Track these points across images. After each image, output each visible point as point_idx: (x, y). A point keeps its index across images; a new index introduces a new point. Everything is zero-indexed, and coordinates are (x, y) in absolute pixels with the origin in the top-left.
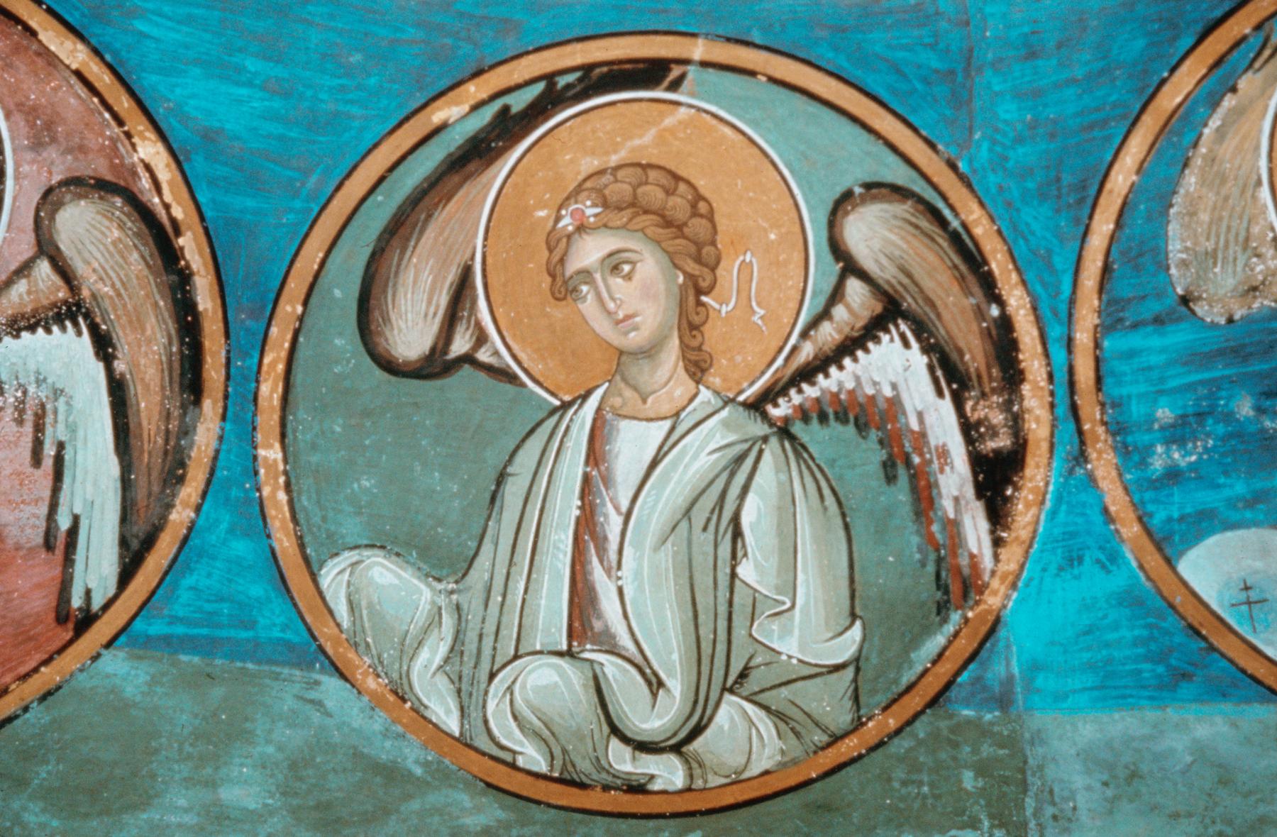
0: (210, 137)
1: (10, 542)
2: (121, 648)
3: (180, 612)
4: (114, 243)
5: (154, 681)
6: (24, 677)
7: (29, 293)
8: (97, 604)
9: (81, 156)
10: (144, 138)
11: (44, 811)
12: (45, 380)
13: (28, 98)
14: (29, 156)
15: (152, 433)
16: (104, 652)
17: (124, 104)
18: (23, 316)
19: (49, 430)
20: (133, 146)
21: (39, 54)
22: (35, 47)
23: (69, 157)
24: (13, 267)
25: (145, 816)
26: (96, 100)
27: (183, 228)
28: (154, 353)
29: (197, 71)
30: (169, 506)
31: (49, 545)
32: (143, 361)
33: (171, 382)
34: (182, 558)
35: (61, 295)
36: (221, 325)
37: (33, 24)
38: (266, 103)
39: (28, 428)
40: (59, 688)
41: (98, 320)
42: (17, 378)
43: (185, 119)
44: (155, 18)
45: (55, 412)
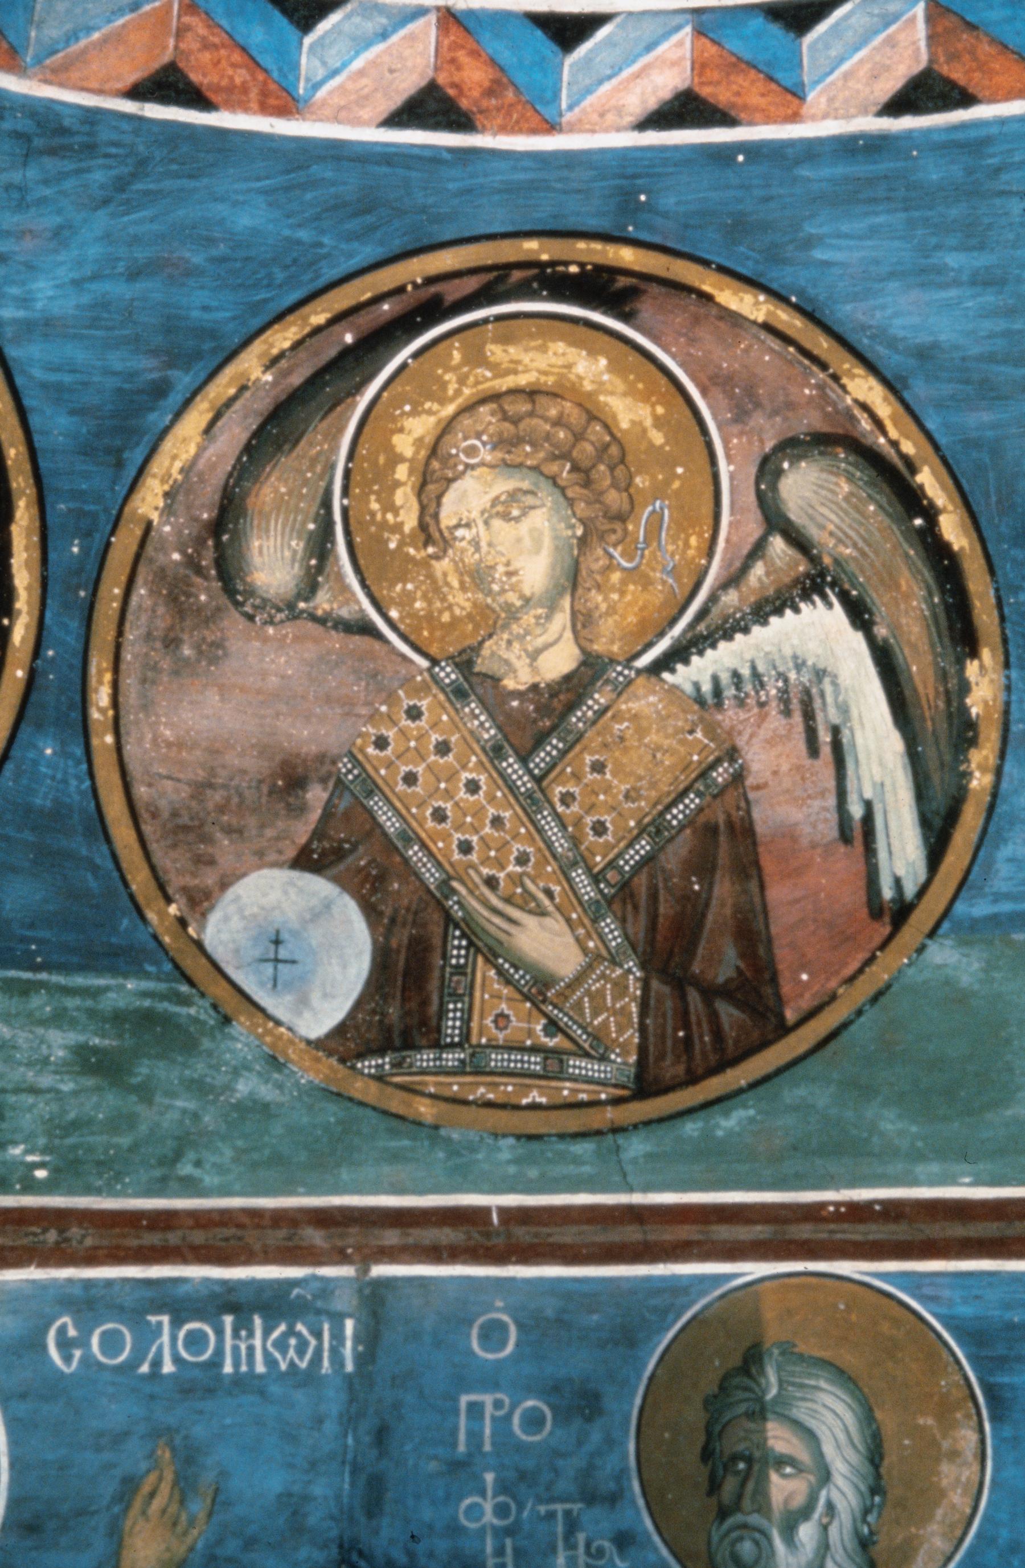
0: (925, 354)
1: (805, 842)
2: (946, 936)
3: (1003, 887)
4: (846, 499)
5: (990, 967)
6: (851, 980)
7: (768, 574)
8: (910, 890)
9: (790, 414)
10: (853, 376)
11: (900, 1116)
12: (804, 663)
13: (720, 368)
14: (735, 429)
15: (931, 697)
16: (929, 942)
17: (822, 345)
18: (767, 600)
19: (820, 717)
20: (843, 387)
21: (721, 318)
22: (714, 311)
23: (778, 419)
24: (745, 551)
25: (1009, 1113)
26: (791, 349)
27: (917, 463)
28: (914, 609)
29: (893, 285)
30: (967, 775)
31: (845, 836)
32: (904, 621)
33: (940, 636)
34: (992, 829)
35: (801, 569)
36: (982, 561)
37: (706, 288)
38: (979, 299)
39: (798, 718)
40: (888, 986)
41: (847, 586)
42: (775, 667)
43: (892, 343)
44: (834, 241)
45: (822, 695)
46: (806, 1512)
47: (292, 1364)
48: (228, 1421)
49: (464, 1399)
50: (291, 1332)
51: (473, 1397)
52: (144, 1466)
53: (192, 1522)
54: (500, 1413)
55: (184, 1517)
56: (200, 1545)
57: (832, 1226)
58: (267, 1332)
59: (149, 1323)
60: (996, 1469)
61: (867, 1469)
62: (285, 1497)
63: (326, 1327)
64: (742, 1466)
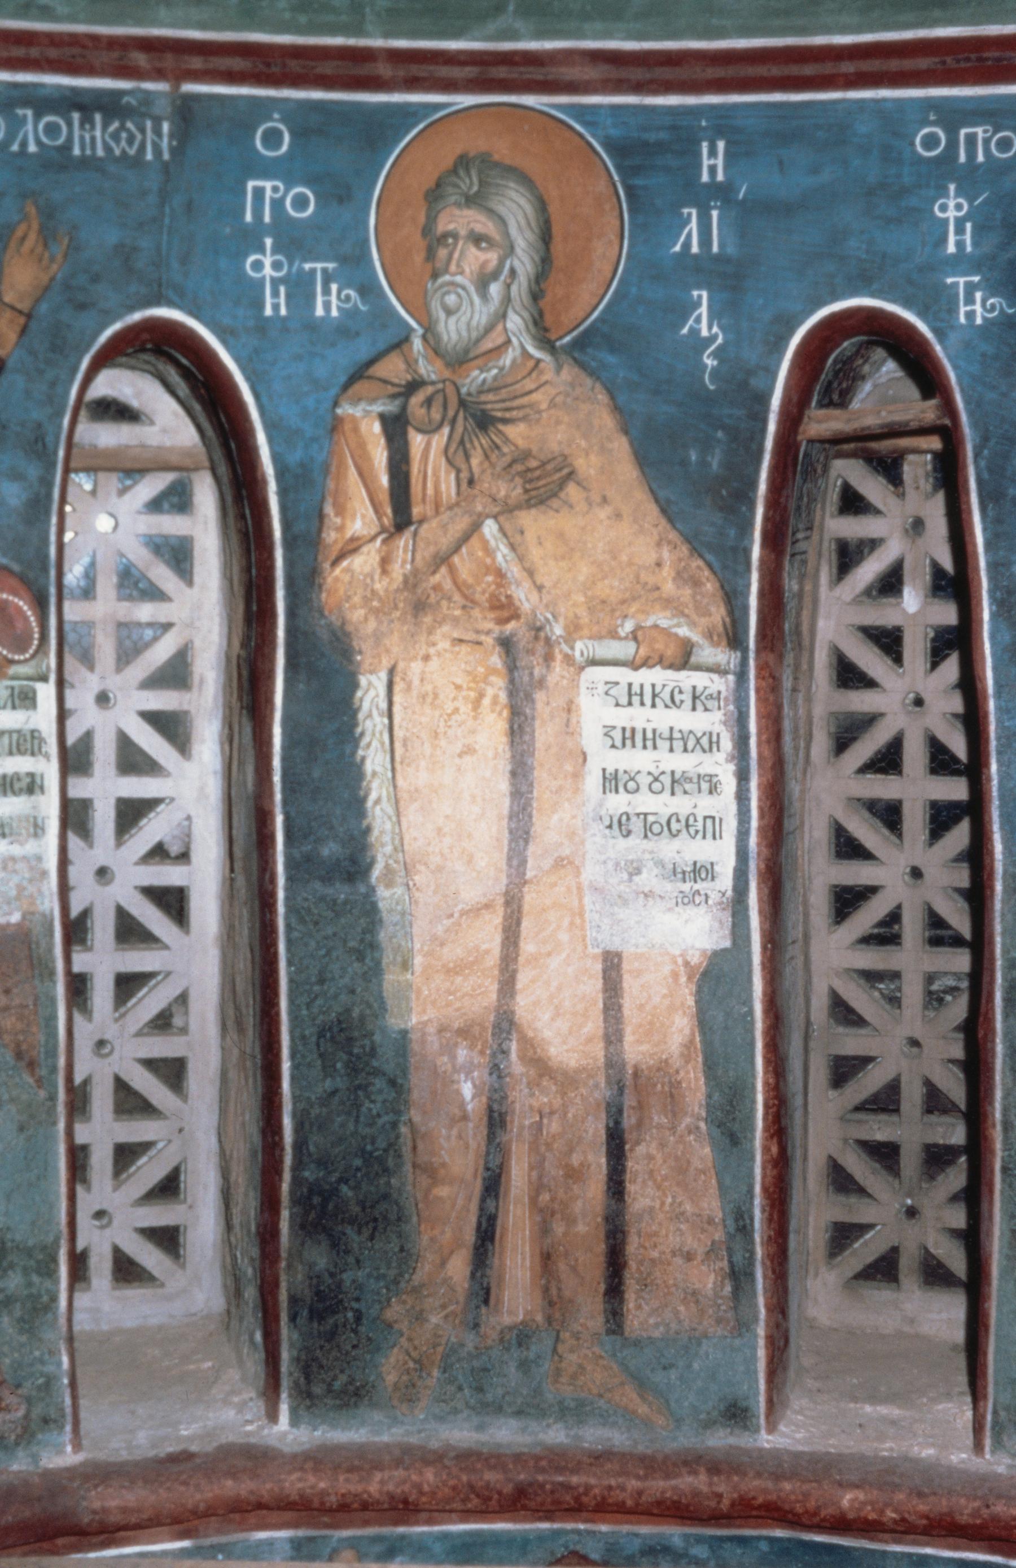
46: (495, 276)
47: (124, 152)
48: (77, 189)
49: (251, 184)
50: (122, 127)
51: (259, 183)
52: (16, 218)
53: (52, 259)
54: (277, 196)
55: (47, 255)
56: (59, 276)
57: (522, 69)
58: (105, 126)
59: (17, 115)
60: (630, 246)
61: (540, 245)
62: (119, 247)
63: (149, 124)
64: (450, 241)
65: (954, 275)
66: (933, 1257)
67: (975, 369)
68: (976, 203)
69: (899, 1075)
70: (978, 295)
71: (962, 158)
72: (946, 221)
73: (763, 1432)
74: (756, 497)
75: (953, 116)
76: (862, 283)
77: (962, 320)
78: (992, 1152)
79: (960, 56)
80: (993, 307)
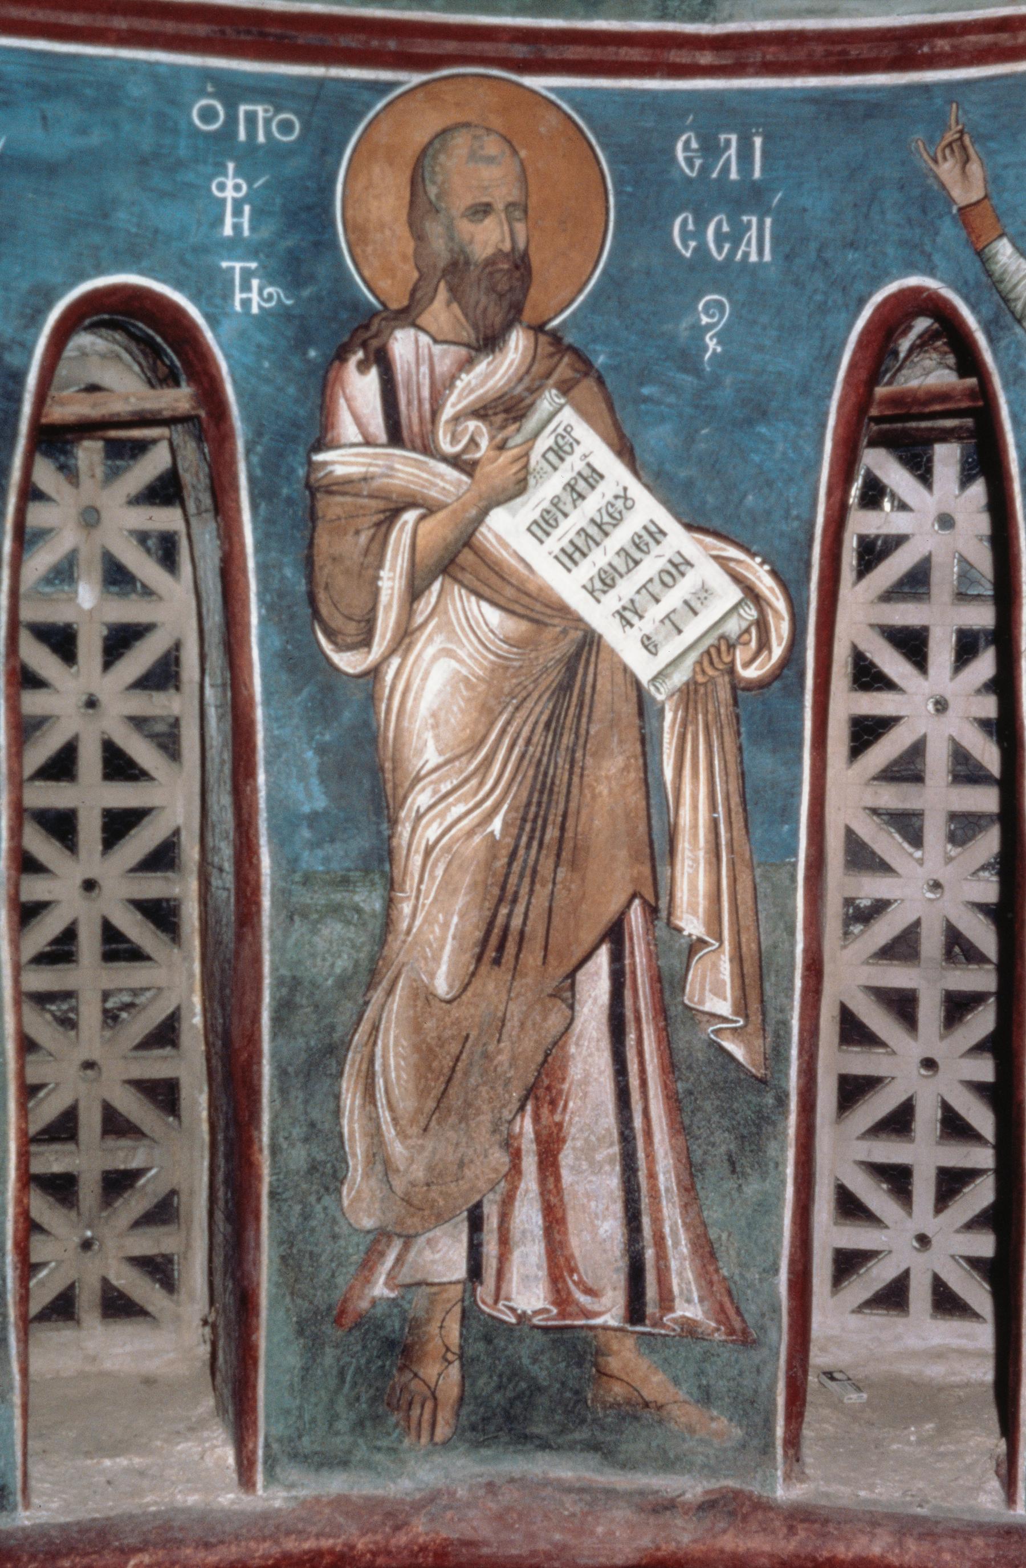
65: (230, 258)
66: (114, 1288)
67: (249, 360)
68: (256, 185)
69: (77, 1101)
70: (255, 283)
71: (242, 136)
72: (223, 201)
73: (20, 1508)
74: (8, 483)
75: (232, 90)
76: (131, 258)
77: (238, 307)
78: (259, 1178)
79: (242, 27)
80: (270, 297)
